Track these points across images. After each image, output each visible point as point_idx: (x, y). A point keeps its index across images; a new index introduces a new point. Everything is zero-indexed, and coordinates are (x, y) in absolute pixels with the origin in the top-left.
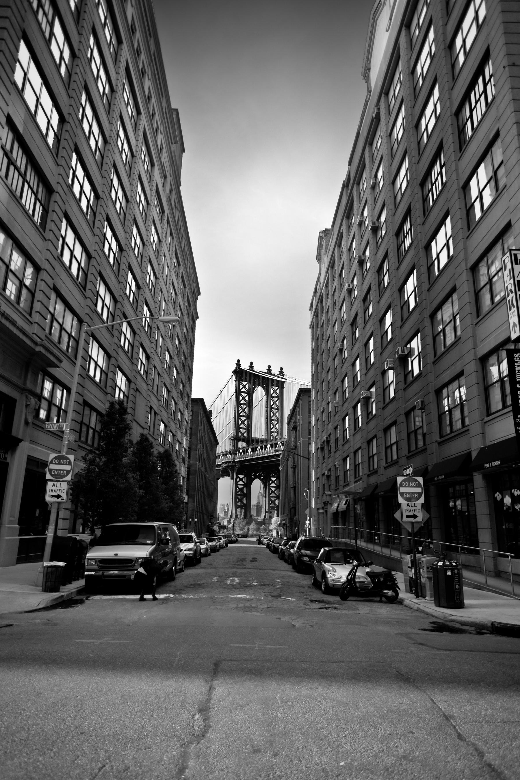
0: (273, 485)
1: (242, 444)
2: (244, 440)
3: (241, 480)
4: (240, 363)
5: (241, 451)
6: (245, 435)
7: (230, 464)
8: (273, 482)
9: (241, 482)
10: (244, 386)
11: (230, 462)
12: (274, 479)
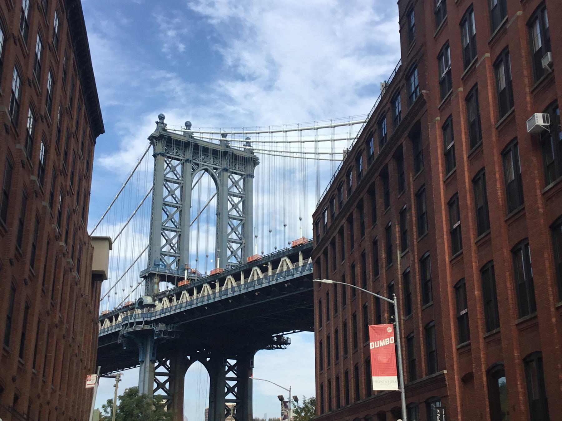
0: (231, 374)
1: (164, 286)
2: (171, 279)
3: (163, 364)
4: (165, 121)
5: (165, 299)
6: (174, 267)
7: (139, 328)
8: (231, 368)
9: (162, 369)
10: (173, 170)
11: (139, 323)
12: (232, 362)
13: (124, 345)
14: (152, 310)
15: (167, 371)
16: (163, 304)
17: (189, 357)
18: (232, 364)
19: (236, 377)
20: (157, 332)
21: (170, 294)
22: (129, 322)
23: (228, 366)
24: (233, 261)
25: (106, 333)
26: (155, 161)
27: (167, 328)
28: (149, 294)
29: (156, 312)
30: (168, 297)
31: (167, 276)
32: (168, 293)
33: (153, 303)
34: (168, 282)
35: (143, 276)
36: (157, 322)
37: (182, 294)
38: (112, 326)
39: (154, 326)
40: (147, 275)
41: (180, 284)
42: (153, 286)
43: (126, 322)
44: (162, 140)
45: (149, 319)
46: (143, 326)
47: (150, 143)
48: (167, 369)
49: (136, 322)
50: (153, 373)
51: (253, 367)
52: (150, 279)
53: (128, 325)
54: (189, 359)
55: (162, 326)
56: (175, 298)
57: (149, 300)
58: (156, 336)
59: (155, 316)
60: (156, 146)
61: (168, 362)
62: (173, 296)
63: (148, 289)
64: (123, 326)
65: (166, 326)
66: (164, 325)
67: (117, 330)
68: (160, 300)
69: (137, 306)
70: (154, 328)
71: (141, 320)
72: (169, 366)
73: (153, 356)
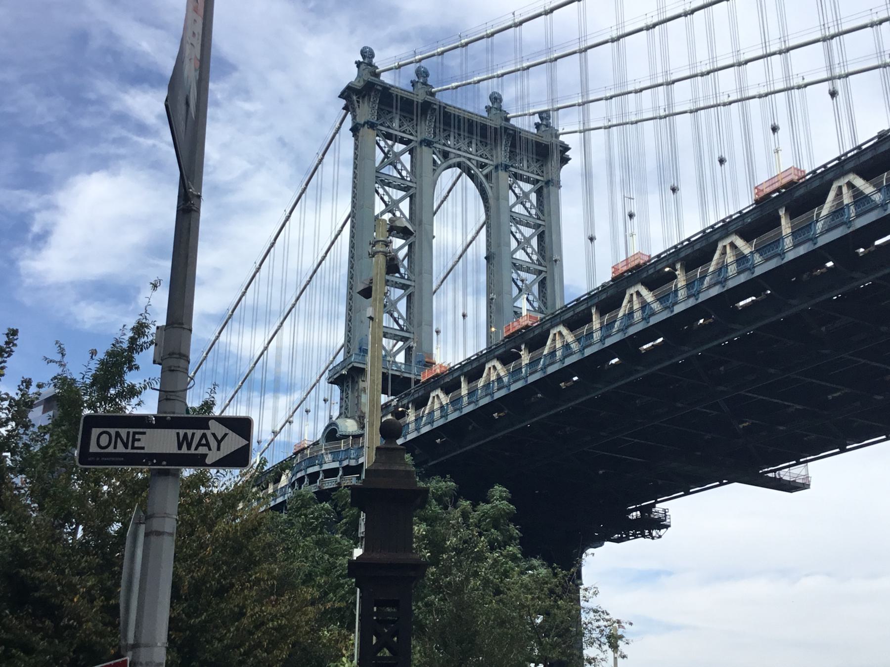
26: (356, 140)
28: (349, 416)
35: (335, 377)
37: (431, 399)
42: (358, 397)
44: (369, 96)
52: (350, 384)
60: (357, 110)
62: (408, 408)
63: (347, 405)
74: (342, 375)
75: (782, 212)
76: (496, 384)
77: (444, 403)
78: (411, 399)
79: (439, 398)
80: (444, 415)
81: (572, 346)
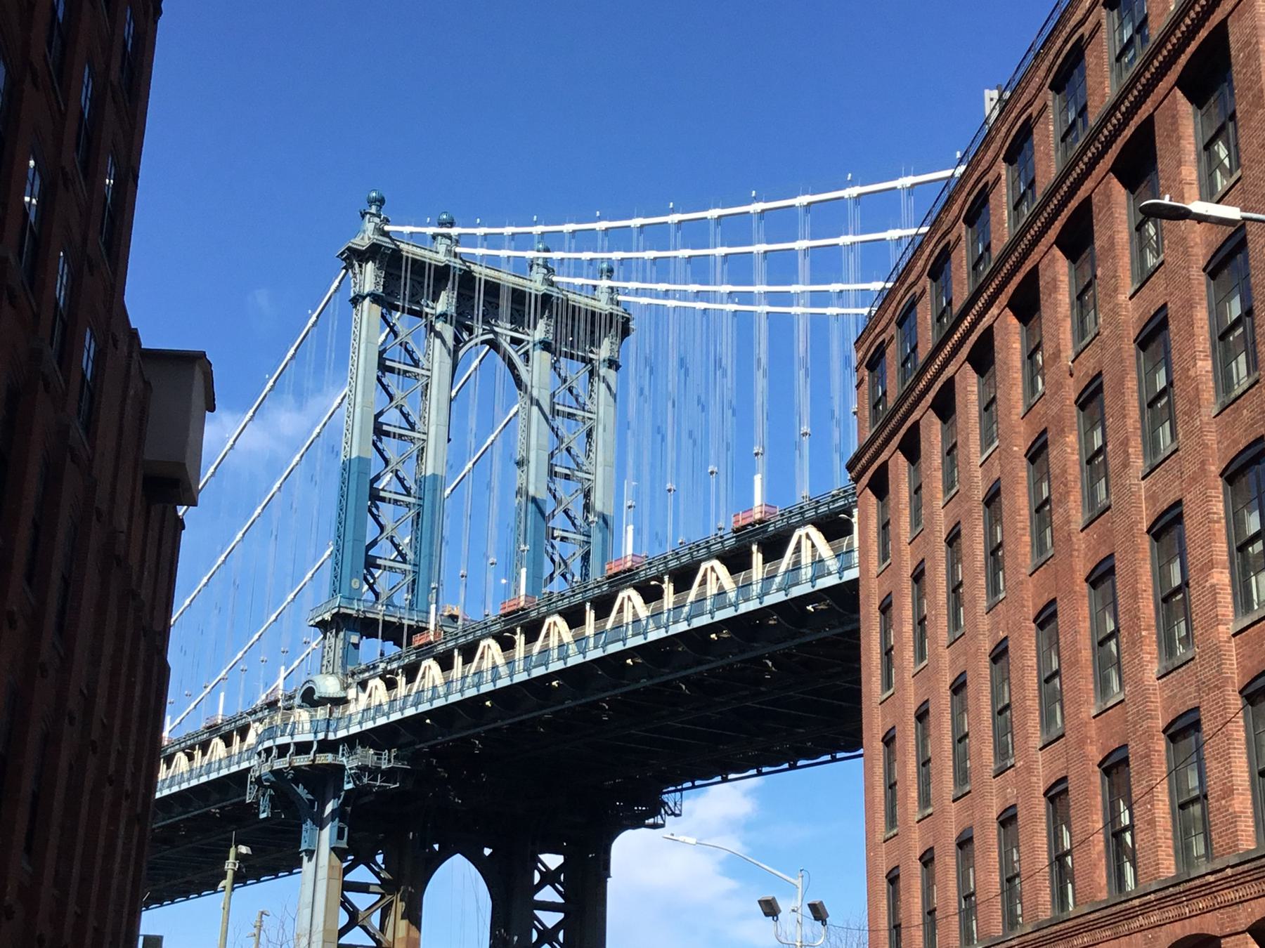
0: (548, 894)
2: (393, 632)
5: (377, 684)
6: (402, 598)
7: (302, 761)
8: (549, 878)
9: (361, 874)
12: (553, 861)
13: (262, 808)
14: (338, 712)
15: (373, 879)
16: (370, 696)
17: (436, 847)
18: (553, 867)
19: (561, 901)
20: (350, 769)
21: (389, 668)
22: (277, 743)
23: (540, 871)
24: (557, 586)
25: (213, 776)
27: (378, 759)
29: (351, 715)
30: (382, 677)
31: (381, 622)
32: (382, 666)
33: (342, 694)
34: (385, 639)
36: (351, 742)
38: (230, 757)
39: (343, 755)
40: (327, 617)
41: (418, 640)
43: (267, 744)
45: (331, 737)
46: (315, 754)
47: (344, 268)
48: (377, 875)
49: (296, 744)
50: (337, 885)
51: (609, 876)
53: (275, 751)
54: (437, 849)
55: (368, 756)
56: (401, 680)
57: (329, 686)
58: (349, 782)
59: (347, 727)
61: (379, 858)
64: (259, 754)
65: (376, 754)
66: (372, 751)
67: (245, 765)
68: (363, 685)
69: (297, 701)
70: (344, 760)
71: (310, 737)
72: (383, 866)
73: (340, 836)
74: (323, 619)
75: (755, 548)
76: (630, 627)
77: (565, 641)
78: (402, 664)
79: (431, 669)
80: (563, 657)
81: (828, 563)
